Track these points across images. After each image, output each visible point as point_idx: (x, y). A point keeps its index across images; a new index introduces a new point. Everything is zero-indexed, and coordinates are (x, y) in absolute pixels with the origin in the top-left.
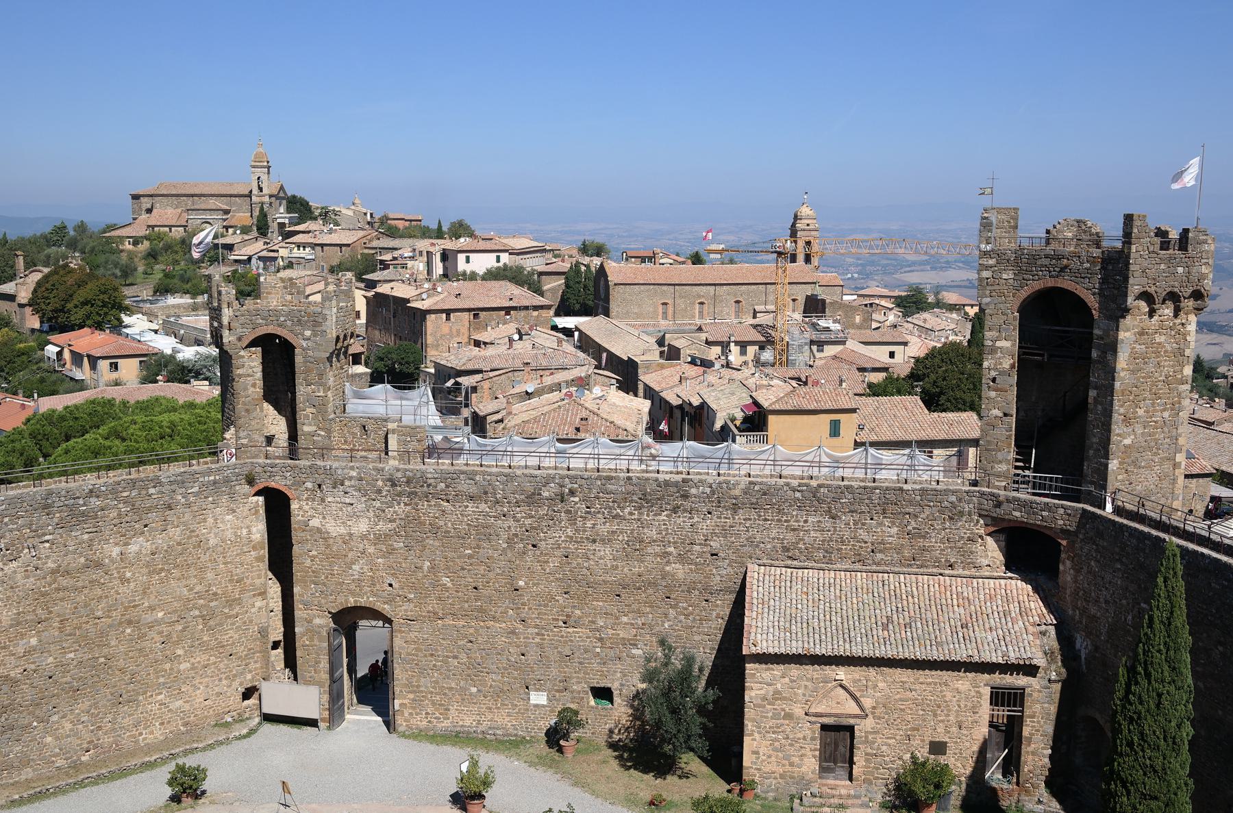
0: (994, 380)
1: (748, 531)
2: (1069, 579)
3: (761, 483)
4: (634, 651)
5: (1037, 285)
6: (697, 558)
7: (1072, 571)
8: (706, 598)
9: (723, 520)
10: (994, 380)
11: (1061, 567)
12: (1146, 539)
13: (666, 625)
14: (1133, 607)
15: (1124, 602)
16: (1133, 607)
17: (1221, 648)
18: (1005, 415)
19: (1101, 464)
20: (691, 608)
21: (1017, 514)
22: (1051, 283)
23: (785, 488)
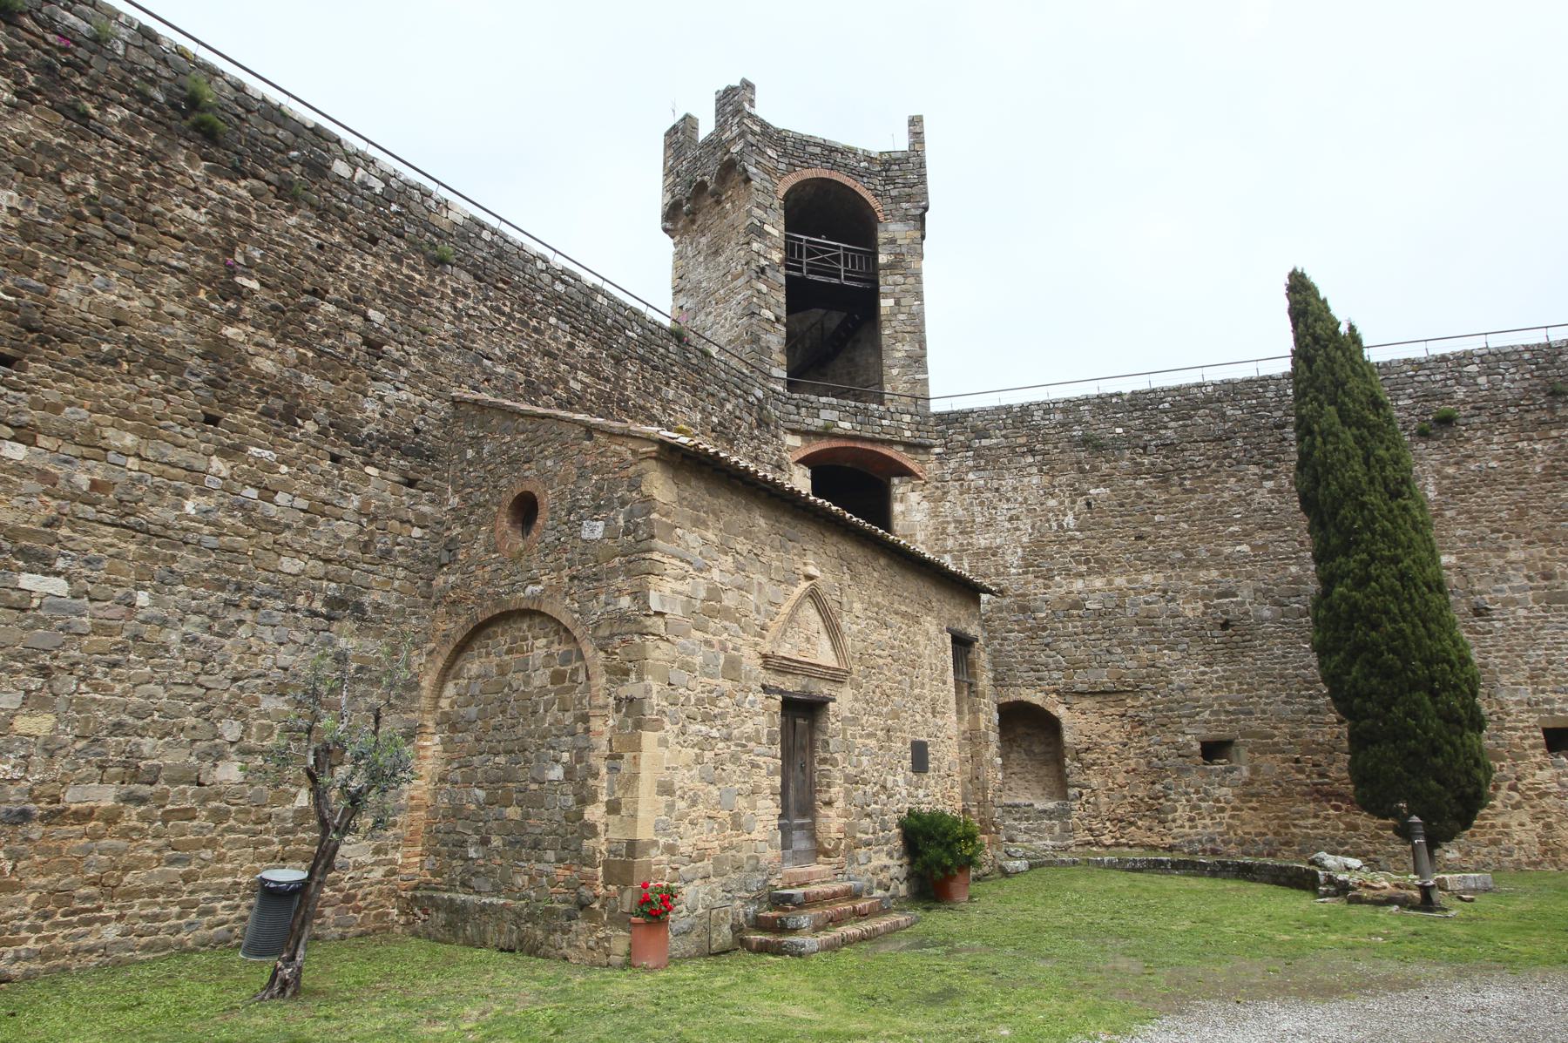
0: (763, 270)
1: (459, 318)
2: (918, 517)
3: (494, 232)
4: (27, 581)
5: (809, 174)
6: (326, 334)
7: (925, 504)
8: (336, 451)
9: (405, 271)
10: (763, 270)
11: (897, 508)
12: (1080, 405)
13: (189, 507)
14: (1073, 502)
15: (1052, 503)
16: (1073, 502)
17: (1269, 484)
18: (778, 319)
19: (916, 382)
20: (284, 469)
21: (846, 425)
22: (825, 174)
23: (540, 265)
